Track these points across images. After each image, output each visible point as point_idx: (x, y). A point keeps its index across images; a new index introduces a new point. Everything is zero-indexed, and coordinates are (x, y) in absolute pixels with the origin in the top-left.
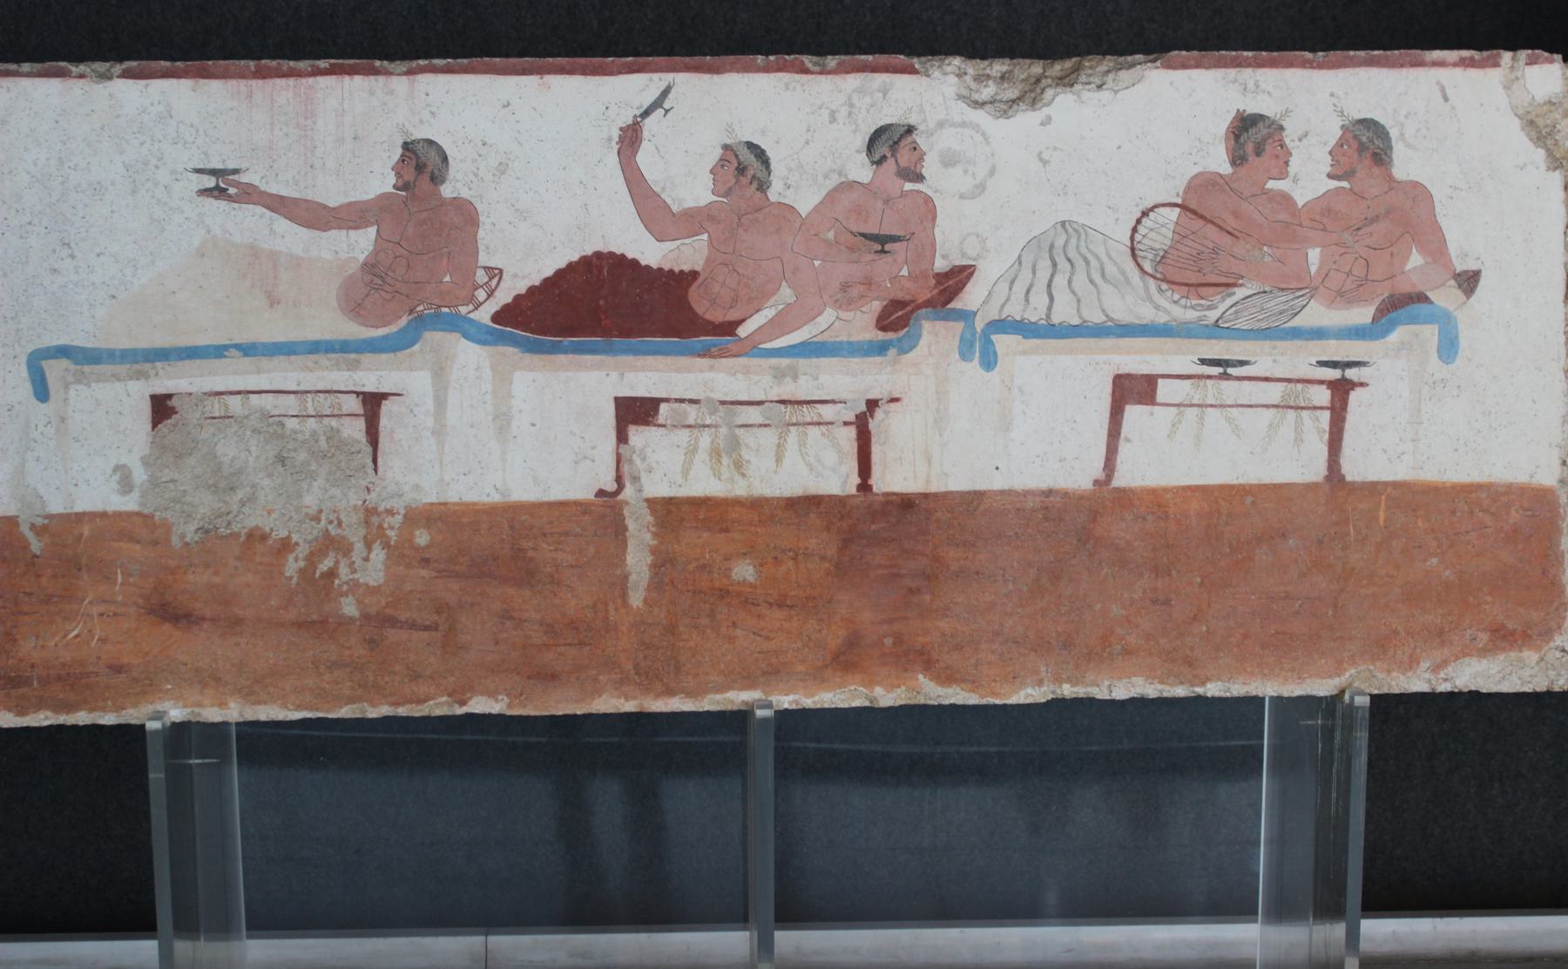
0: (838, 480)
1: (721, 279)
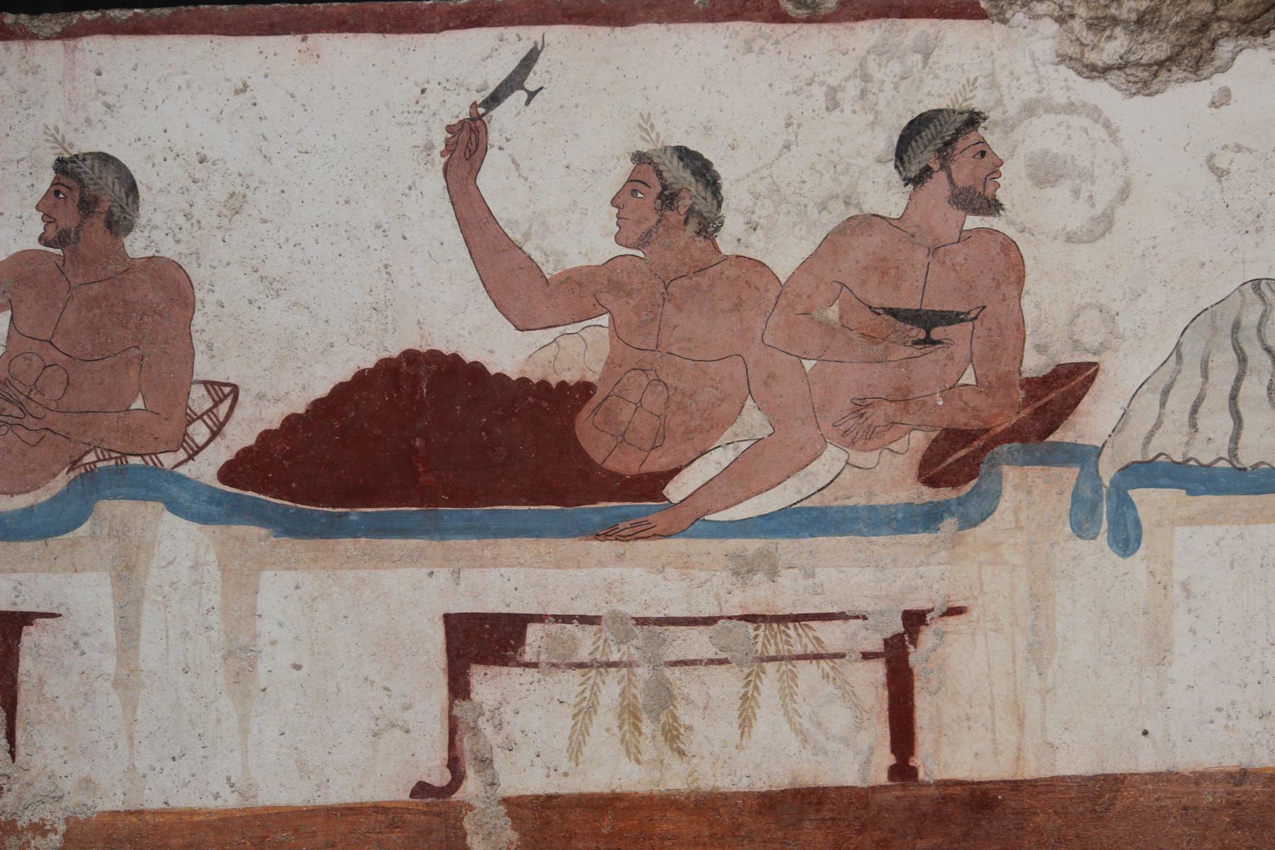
0: (849, 755)
1: (634, 396)
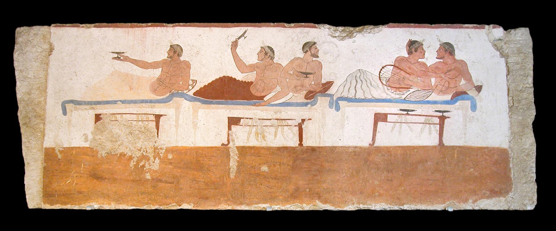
0: (293, 142)
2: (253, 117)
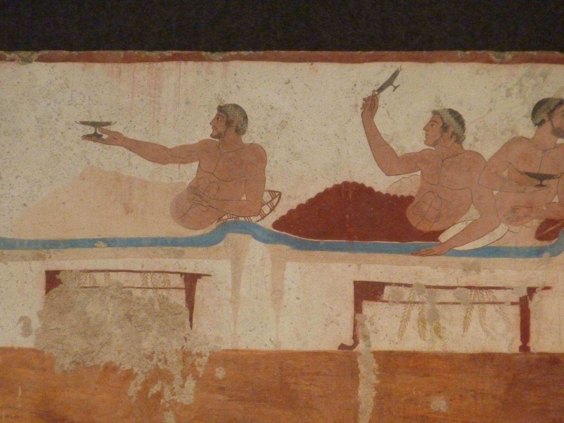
0: (505, 342)
2: (413, 282)
